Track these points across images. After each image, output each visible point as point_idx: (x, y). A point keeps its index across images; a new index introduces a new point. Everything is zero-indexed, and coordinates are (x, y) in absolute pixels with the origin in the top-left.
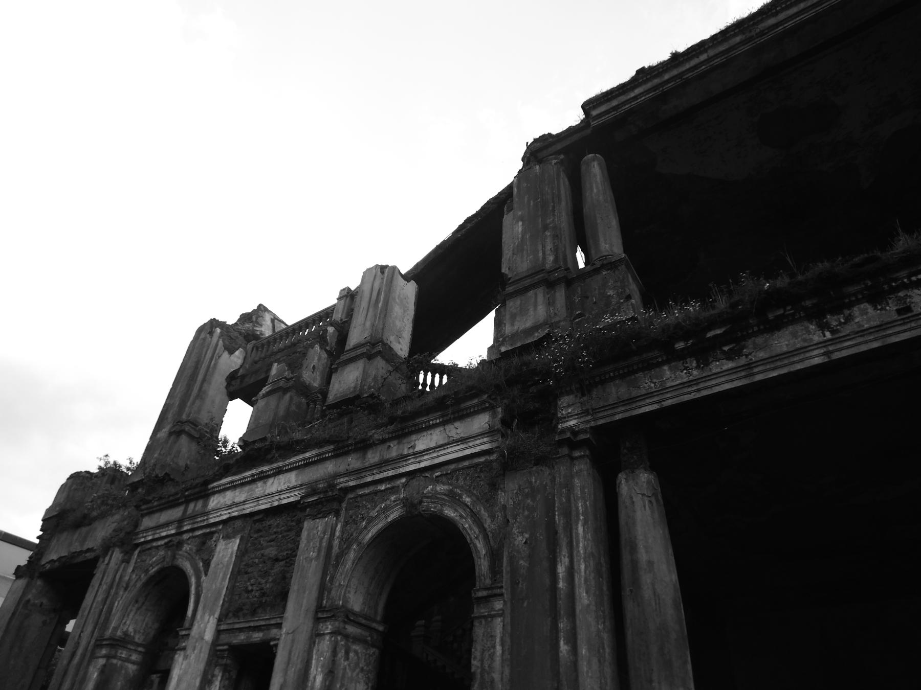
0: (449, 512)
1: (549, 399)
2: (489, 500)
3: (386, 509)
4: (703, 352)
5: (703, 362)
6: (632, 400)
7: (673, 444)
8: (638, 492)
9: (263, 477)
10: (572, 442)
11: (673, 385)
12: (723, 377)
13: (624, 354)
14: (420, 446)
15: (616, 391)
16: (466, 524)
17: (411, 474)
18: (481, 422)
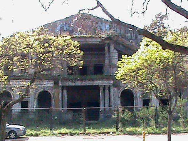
0: (48, 91)
1: (58, 82)
2: (53, 91)
3: (41, 89)
4: (72, 81)
5: (72, 82)
6: (66, 84)
7: (69, 88)
8: (65, 92)
9: (20, 81)
10: (61, 86)
11: (69, 84)
12: (73, 84)
13: (65, 79)
14: (45, 83)
15: (65, 82)
16: (50, 92)
17: (43, 86)
18: (52, 82)
